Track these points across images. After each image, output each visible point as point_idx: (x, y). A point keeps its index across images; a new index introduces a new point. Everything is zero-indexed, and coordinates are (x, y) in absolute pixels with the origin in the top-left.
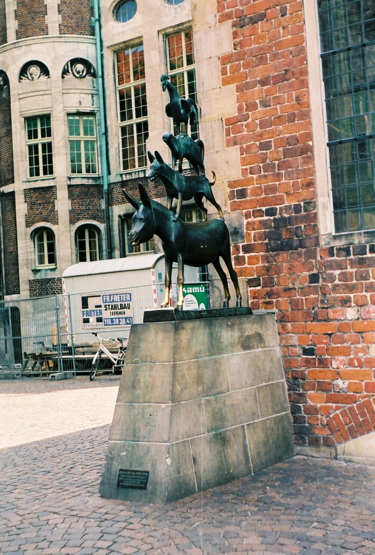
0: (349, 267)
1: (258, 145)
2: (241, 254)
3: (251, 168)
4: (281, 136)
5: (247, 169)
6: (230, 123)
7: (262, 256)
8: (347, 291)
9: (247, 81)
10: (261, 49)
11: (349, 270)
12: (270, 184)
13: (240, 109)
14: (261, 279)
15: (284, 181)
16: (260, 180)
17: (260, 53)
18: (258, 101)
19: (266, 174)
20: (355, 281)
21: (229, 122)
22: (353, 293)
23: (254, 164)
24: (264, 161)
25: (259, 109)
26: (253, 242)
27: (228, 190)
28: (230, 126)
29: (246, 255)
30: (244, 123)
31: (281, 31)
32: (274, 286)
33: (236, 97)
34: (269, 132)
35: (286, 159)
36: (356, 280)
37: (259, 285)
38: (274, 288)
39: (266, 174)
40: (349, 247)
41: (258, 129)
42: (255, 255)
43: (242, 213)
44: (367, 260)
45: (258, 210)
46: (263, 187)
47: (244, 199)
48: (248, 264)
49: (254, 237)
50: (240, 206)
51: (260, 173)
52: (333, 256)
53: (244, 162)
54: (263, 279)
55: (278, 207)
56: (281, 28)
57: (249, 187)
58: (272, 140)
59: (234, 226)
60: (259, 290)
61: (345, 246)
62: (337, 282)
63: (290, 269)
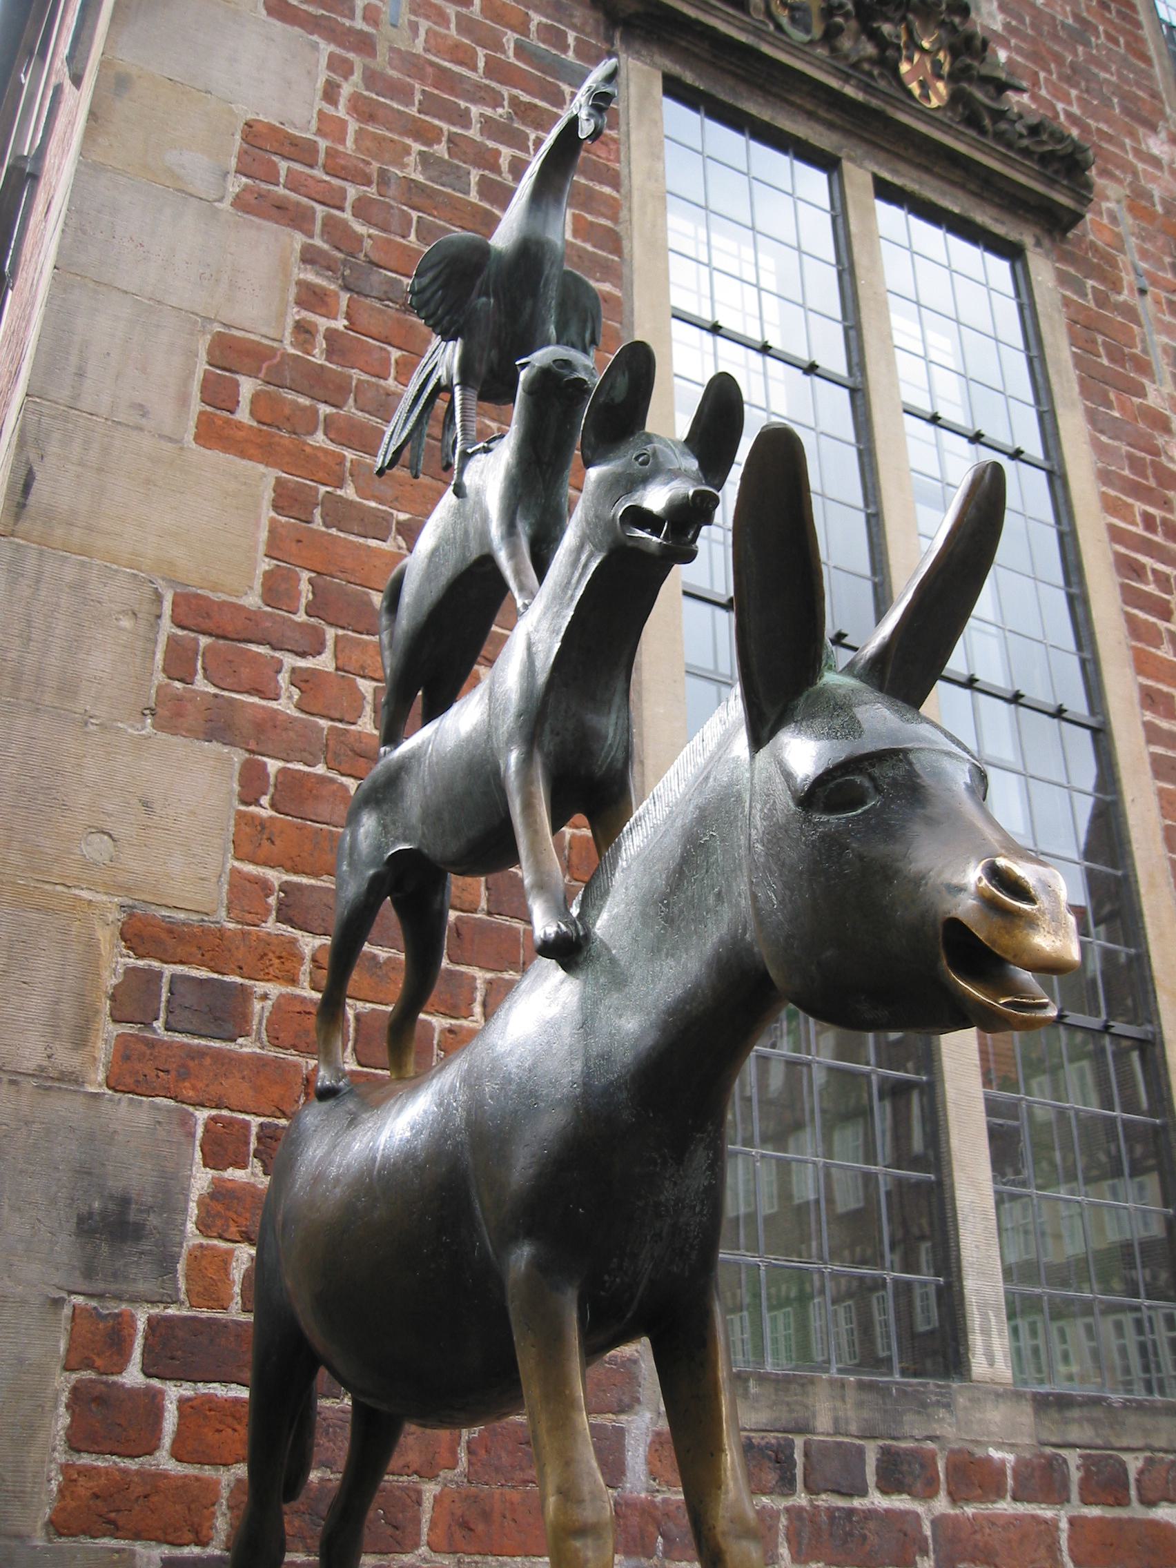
2: (133, 1376)
3: (286, 887)
5: (265, 887)
6: (208, 624)
9: (339, 492)
13: (277, 589)
21: (195, 612)
23: (316, 875)
27: (117, 963)
28: (204, 641)
29: (174, 1392)
33: (265, 524)
35: (499, 919)
40: (791, 1445)
43: (186, 1122)
44: (872, 1525)
47: (216, 1044)
48: (177, 1455)
50: (184, 1074)
53: (252, 839)
57: (260, 987)
59: (115, 1185)
61: (772, 1438)
63: (466, 1526)
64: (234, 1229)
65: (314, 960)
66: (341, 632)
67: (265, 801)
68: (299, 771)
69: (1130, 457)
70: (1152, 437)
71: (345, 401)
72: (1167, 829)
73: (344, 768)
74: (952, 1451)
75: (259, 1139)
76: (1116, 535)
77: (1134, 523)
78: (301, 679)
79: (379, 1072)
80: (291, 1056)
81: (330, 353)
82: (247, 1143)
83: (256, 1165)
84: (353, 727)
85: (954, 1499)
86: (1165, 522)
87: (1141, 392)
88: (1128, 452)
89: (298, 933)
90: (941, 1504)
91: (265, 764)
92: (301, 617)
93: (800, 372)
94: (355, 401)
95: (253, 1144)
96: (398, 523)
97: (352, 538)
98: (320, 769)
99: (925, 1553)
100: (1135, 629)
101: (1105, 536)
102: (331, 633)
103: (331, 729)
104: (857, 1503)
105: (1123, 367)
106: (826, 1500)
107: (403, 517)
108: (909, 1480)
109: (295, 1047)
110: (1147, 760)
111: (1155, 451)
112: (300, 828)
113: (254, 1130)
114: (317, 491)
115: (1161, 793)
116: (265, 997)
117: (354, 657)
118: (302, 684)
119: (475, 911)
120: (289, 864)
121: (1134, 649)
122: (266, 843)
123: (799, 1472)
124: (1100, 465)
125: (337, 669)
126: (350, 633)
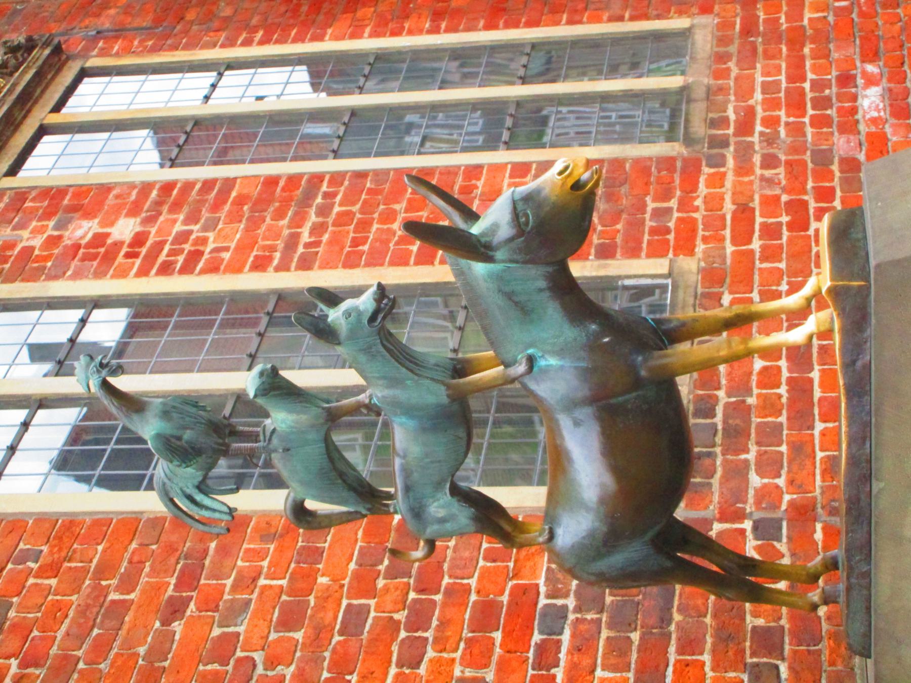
0: (743, 456)
1: (342, 638)
3: (400, 665)
4: (346, 582)
5: (397, 675)
7: (681, 651)
8: (808, 463)
10: (83, 611)
11: (751, 456)
12: (467, 616)
14: (755, 660)
15: (473, 582)
16: (448, 638)
17: (92, 617)
18: (216, 632)
19: (435, 623)
20: (784, 448)
22: (814, 451)
23: (391, 653)
24: (395, 626)
25: (241, 629)
26: (631, 675)
30: (260, 670)
31: (73, 565)
32: (783, 627)
34: (320, 607)
36: (780, 445)
37: (777, 667)
38: (787, 626)
39: (435, 623)
41: (299, 635)
42: (674, 672)
44: (731, 421)
45: (535, 651)
46: (470, 635)
49: (615, 668)
51: (426, 639)
52: (710, 485)
54: (753, 655)
55: (543, 601)
56: (67, 564)
57: (457, 672)
58: (345, 602)
60: (791, 668)
62: (781, 482)
64: (588, 678)
65: (441, 652)
66: (238, 650)
67: (348, 677)
68: (329, 664)
69: (83, 260)
70: (66, 246)
71: (75, 655)
72: (345, 266)
73: (326, 642)
74: (695, 387)
75: (540, 670)
76: (143, 272)
77: (133, 264)
78: (271, 663)
79: (502, 622)
80: (495, 659)
81: (37, 665)
82: (542, 675)
83: (553, 671)
84: (300, 641)
85: (718, 388)
86: (130, 246)
87: (28, 251)
88: (79, 261)
89: (426, 659)
90: (721, 394)
91: (326, 679)
92: (230, 668)
93: (26, 434)
94: (73, 651)
95: (544, 672)
96: (163, 624)
97: (174, 646)
98: (327, 654)
99: (744, 402)
100: (213, 268)
101: (144, 280)
102: (239, 654)
103: (302, 650)
104: (720, 427)
105: (11, 256)
106: (719, 439)
107: (157, 624)
108: (708, 405)
109: (490, 657)
110: (300, 272)
111: (77, 247)
112: (364, 660)
113: (535, 672)
114: (141, 665)
115: (321, 267)
116: (462, 672)
117: (255, 642)
118: (274, 665)
119: (409, 584)
120: (386, 664)
121: (225, 272)
122: (374, 675)
123: (705, 450)
124: (90, 276)
125: (263, 649)
126: (239, 645)
